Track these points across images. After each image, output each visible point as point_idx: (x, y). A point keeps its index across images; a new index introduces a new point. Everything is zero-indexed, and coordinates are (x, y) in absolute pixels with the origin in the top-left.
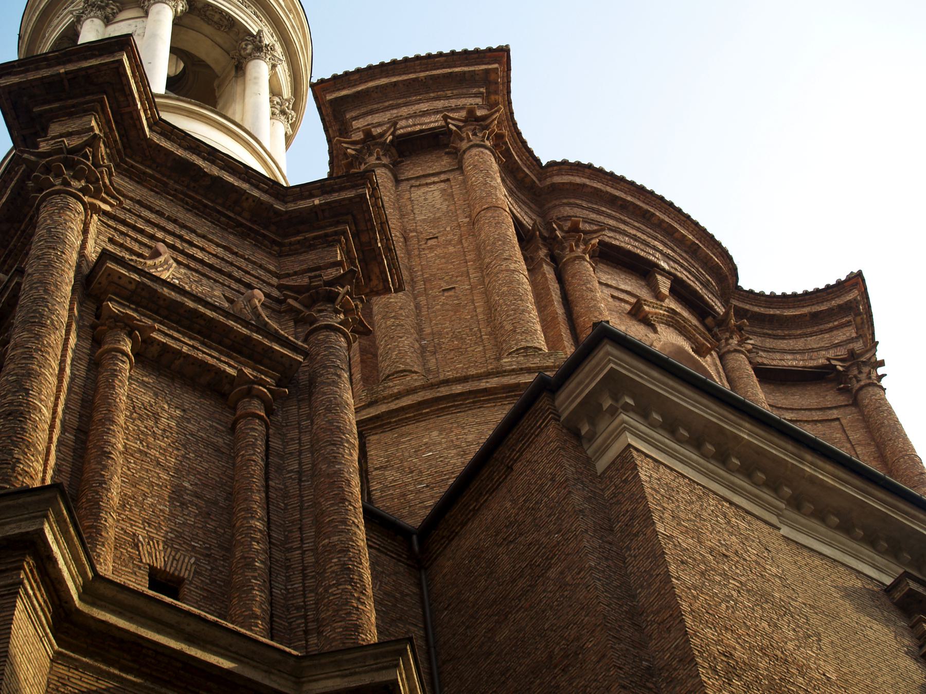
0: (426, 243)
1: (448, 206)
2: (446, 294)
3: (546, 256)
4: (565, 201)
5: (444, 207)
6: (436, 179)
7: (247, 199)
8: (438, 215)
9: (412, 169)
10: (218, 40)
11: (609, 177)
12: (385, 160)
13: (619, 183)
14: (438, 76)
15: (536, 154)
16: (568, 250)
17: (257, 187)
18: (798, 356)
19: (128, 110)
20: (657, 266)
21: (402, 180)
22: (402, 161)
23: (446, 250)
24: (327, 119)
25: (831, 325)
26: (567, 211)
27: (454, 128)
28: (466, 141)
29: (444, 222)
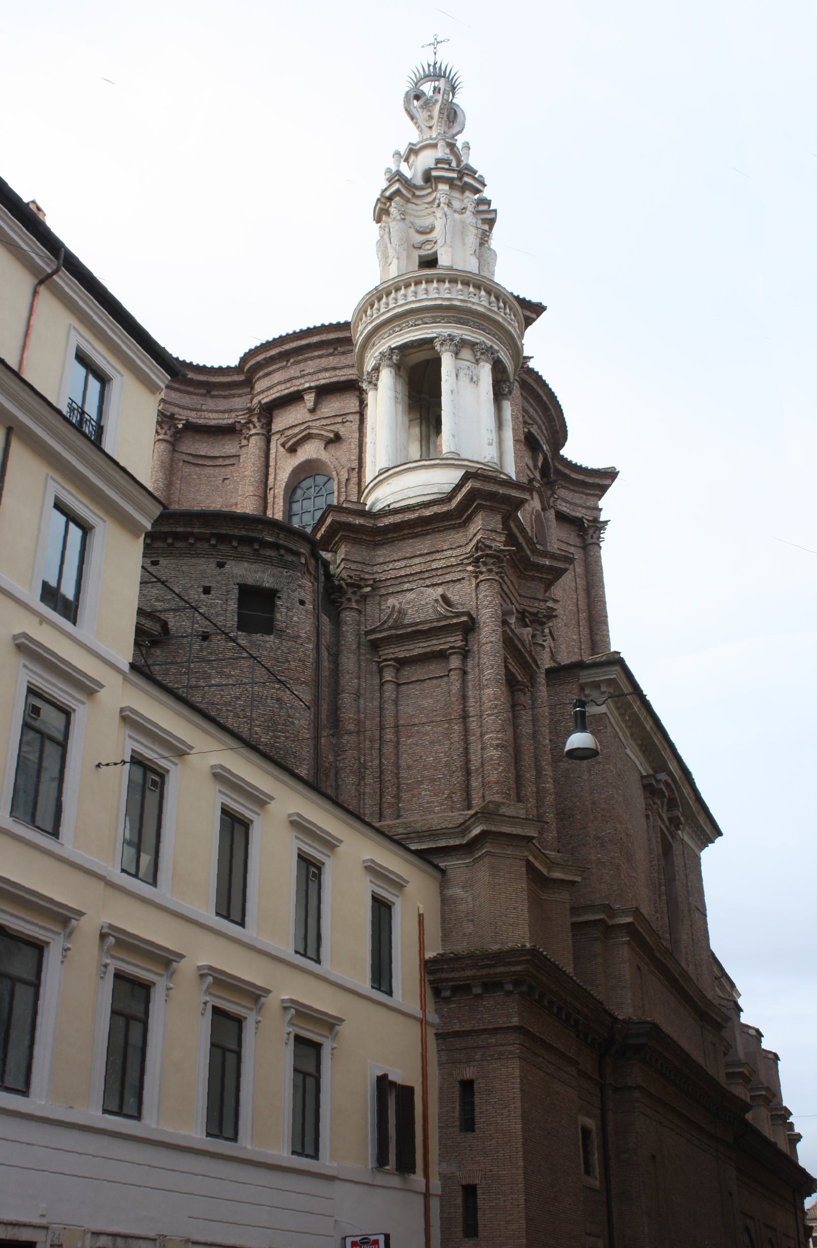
18: (568, 505)
20: (542, 448)
25: (588, 492)
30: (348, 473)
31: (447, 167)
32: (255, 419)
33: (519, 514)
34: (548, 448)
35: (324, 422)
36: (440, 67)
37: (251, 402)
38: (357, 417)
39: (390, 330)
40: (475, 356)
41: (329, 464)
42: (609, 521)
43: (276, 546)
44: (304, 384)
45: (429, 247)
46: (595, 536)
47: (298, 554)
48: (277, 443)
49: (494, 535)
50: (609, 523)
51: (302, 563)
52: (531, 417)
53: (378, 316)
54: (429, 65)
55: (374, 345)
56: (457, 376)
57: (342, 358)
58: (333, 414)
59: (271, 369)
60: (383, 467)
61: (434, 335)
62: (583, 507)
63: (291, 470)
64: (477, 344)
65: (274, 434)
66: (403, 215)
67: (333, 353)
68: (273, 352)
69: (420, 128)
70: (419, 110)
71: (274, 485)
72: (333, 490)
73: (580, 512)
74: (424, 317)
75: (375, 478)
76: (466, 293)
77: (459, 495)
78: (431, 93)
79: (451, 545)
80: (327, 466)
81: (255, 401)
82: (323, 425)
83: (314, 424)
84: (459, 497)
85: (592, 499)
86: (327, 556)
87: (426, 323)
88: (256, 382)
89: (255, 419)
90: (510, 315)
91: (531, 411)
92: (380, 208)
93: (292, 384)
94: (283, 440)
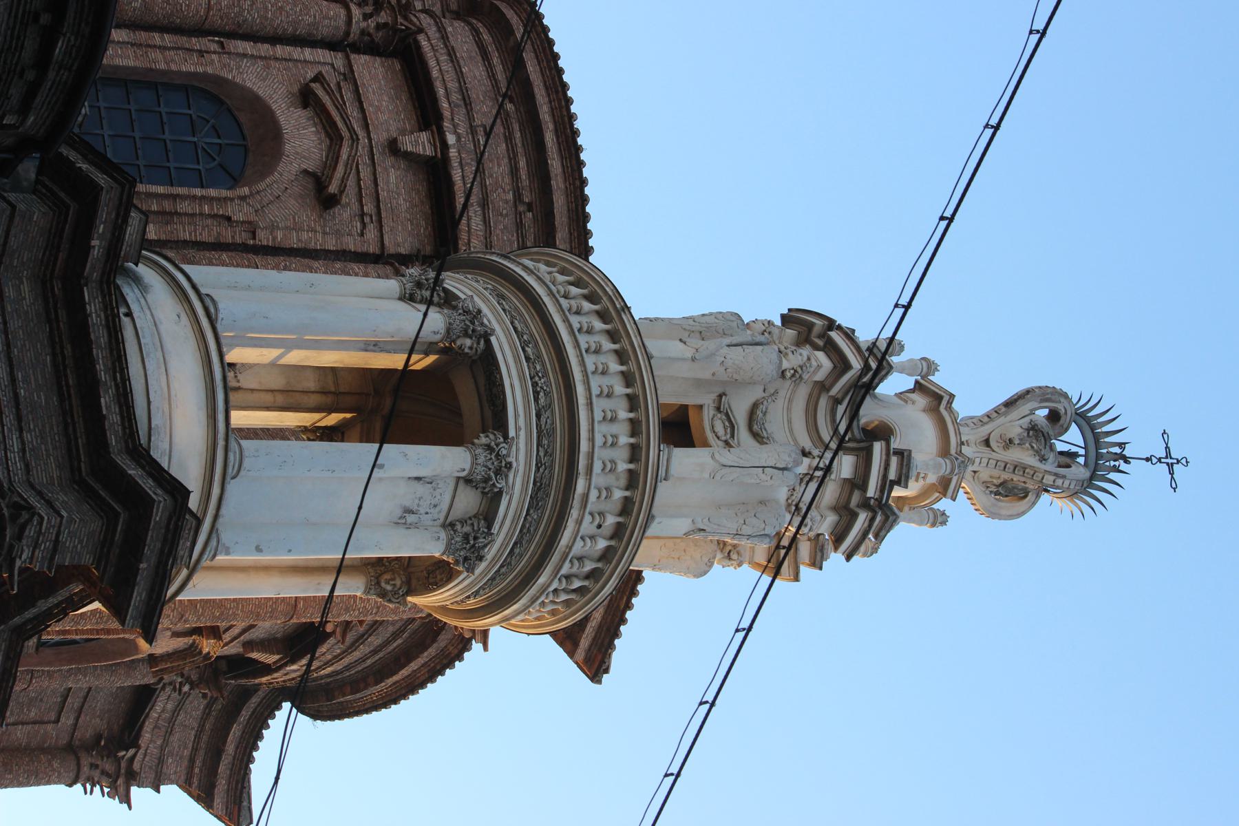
11: (438, 668)
13: (428, 672)
25: (198, 763)
30: (243, 222)
31: (892, 475)
32: (383, 17)
33: (96, 605)
34: (293, 675)
35: (365, 173)
36: (1117, 470)
37: (422, 11)
38: (373, 248)
39: (532, 335)
40: (463, 522)
41: (268, 180)
42: (130, 807)
43: (43, 60)
44: (455, 133)
45: (719, 428)
46: (96, 774)
47: (25, 108)
48: (325, 63)
49: (46, 545)
50: (125, 806)
51: (3, 117)
52: (361, 639)
53: (563, 311)
54: (1122, 445)
55: (501, 297)
56: (418, 479)
57: (509, 221)
58: (383, 194)
59: (496, 61)
60: (221, 306)
61: (512, 433)
62: (162, 748)
63: (260, 93)
64: (489, 527)
65: (348, 57)
66: (793, 375)
67: (521, 201)
68: (532, 68)
69: (986, 419)
70: (1027, 419)
71: (229, 53)
72: (207, 188)
73: (151, 741)
74: (553, 413)
75: (194, 287)
76: (603, 506)
77: (140, 472)
78: (1060, 447)
79: (32, 450)
80: (263, 176)
81: (426, 20)
82: (358, 172)
83: (362, 150)
84: (134, 472)
85: (182, 769)
86: (28, 169)
87: (538, 416)
88: (469, 24)
89: (383, 17)
90: (553, 602)
91: (375, 641)
92: (812, 325)
93: (457, 106)
94: (332, 80)
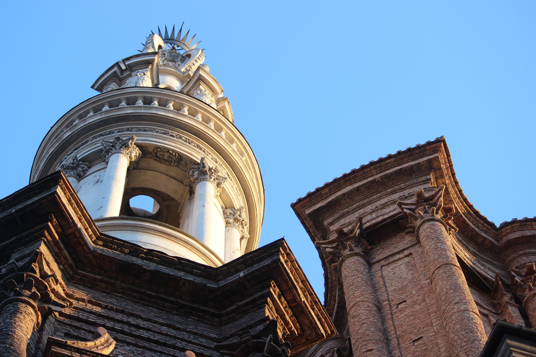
0: (397, 308)
1: (413, 274)
2: (416, 344)
3: (511, 299)
4: (521, 252)
5: (410, 276)
6: (401, 256)
7: (184, 284)
8: (405, 284)
9: (381, 253)
10: (173, 174)
12: (357, 250)
14: (391, 174)
15: (490, 220)
16: (528, 290)
17: (191, 273)
19: (70, 231)
21: (374, 263)
22: (372, 249)
23: (413, 310)
24: (311, 230)
26: (524, 260)
27: (408, 211)
28: (419, 219)
29: (410, 287)
